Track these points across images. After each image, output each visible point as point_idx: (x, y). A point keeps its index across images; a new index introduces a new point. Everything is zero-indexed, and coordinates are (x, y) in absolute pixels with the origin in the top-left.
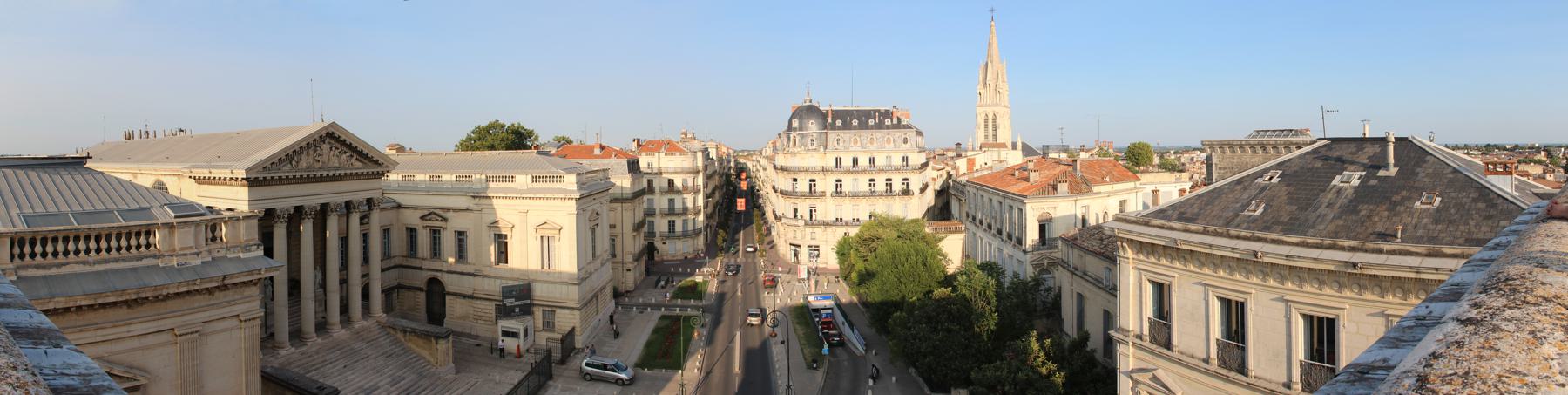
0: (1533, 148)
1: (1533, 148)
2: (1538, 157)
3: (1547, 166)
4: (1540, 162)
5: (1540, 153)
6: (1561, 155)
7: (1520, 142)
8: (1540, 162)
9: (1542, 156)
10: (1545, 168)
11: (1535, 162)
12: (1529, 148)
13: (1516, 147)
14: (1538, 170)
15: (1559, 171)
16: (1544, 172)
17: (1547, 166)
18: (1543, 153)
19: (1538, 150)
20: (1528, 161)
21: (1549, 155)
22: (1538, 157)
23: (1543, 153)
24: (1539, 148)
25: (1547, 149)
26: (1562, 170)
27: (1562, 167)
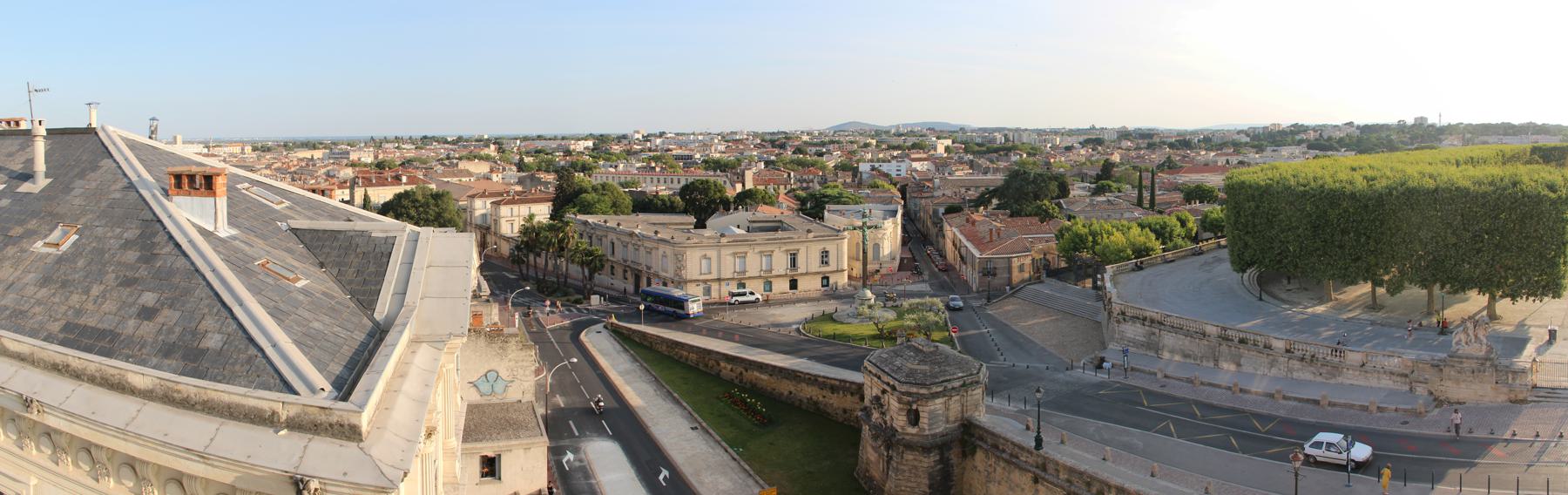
0: (481, 141)
1: (481, 141)
2: (486, 151)
3: (496, 162)
4: (487, 158)
5: (488, 146)
6: (515, 150)
7: (465, 133)
8: (487, 158)
9: (492, 150)
10: (493, 165)
11: (481, 158)
12: (477, 141)
13: (460, 139)
14: (481, 168)
15: (511, 170)
16: (492, 171)
17: (496, 162)
18: (492, 147)
19: (487, 143)
20: (471, 157)
21: (501, 150)
22: (486, 151)
23: (492, 147)
24: (488, 140)
25: (498, 142)
26: (514, 168)
27: (515, 165)
